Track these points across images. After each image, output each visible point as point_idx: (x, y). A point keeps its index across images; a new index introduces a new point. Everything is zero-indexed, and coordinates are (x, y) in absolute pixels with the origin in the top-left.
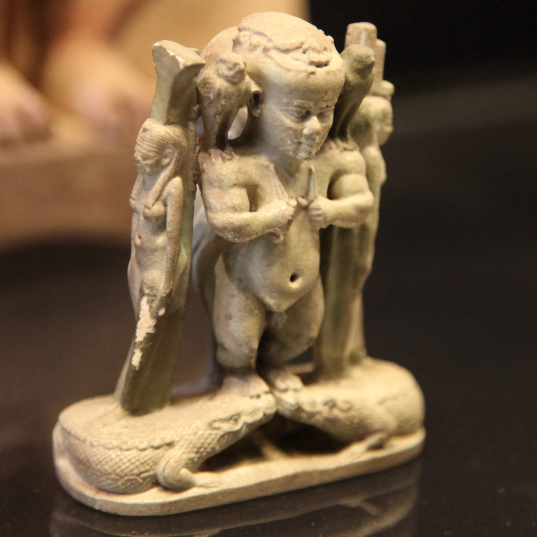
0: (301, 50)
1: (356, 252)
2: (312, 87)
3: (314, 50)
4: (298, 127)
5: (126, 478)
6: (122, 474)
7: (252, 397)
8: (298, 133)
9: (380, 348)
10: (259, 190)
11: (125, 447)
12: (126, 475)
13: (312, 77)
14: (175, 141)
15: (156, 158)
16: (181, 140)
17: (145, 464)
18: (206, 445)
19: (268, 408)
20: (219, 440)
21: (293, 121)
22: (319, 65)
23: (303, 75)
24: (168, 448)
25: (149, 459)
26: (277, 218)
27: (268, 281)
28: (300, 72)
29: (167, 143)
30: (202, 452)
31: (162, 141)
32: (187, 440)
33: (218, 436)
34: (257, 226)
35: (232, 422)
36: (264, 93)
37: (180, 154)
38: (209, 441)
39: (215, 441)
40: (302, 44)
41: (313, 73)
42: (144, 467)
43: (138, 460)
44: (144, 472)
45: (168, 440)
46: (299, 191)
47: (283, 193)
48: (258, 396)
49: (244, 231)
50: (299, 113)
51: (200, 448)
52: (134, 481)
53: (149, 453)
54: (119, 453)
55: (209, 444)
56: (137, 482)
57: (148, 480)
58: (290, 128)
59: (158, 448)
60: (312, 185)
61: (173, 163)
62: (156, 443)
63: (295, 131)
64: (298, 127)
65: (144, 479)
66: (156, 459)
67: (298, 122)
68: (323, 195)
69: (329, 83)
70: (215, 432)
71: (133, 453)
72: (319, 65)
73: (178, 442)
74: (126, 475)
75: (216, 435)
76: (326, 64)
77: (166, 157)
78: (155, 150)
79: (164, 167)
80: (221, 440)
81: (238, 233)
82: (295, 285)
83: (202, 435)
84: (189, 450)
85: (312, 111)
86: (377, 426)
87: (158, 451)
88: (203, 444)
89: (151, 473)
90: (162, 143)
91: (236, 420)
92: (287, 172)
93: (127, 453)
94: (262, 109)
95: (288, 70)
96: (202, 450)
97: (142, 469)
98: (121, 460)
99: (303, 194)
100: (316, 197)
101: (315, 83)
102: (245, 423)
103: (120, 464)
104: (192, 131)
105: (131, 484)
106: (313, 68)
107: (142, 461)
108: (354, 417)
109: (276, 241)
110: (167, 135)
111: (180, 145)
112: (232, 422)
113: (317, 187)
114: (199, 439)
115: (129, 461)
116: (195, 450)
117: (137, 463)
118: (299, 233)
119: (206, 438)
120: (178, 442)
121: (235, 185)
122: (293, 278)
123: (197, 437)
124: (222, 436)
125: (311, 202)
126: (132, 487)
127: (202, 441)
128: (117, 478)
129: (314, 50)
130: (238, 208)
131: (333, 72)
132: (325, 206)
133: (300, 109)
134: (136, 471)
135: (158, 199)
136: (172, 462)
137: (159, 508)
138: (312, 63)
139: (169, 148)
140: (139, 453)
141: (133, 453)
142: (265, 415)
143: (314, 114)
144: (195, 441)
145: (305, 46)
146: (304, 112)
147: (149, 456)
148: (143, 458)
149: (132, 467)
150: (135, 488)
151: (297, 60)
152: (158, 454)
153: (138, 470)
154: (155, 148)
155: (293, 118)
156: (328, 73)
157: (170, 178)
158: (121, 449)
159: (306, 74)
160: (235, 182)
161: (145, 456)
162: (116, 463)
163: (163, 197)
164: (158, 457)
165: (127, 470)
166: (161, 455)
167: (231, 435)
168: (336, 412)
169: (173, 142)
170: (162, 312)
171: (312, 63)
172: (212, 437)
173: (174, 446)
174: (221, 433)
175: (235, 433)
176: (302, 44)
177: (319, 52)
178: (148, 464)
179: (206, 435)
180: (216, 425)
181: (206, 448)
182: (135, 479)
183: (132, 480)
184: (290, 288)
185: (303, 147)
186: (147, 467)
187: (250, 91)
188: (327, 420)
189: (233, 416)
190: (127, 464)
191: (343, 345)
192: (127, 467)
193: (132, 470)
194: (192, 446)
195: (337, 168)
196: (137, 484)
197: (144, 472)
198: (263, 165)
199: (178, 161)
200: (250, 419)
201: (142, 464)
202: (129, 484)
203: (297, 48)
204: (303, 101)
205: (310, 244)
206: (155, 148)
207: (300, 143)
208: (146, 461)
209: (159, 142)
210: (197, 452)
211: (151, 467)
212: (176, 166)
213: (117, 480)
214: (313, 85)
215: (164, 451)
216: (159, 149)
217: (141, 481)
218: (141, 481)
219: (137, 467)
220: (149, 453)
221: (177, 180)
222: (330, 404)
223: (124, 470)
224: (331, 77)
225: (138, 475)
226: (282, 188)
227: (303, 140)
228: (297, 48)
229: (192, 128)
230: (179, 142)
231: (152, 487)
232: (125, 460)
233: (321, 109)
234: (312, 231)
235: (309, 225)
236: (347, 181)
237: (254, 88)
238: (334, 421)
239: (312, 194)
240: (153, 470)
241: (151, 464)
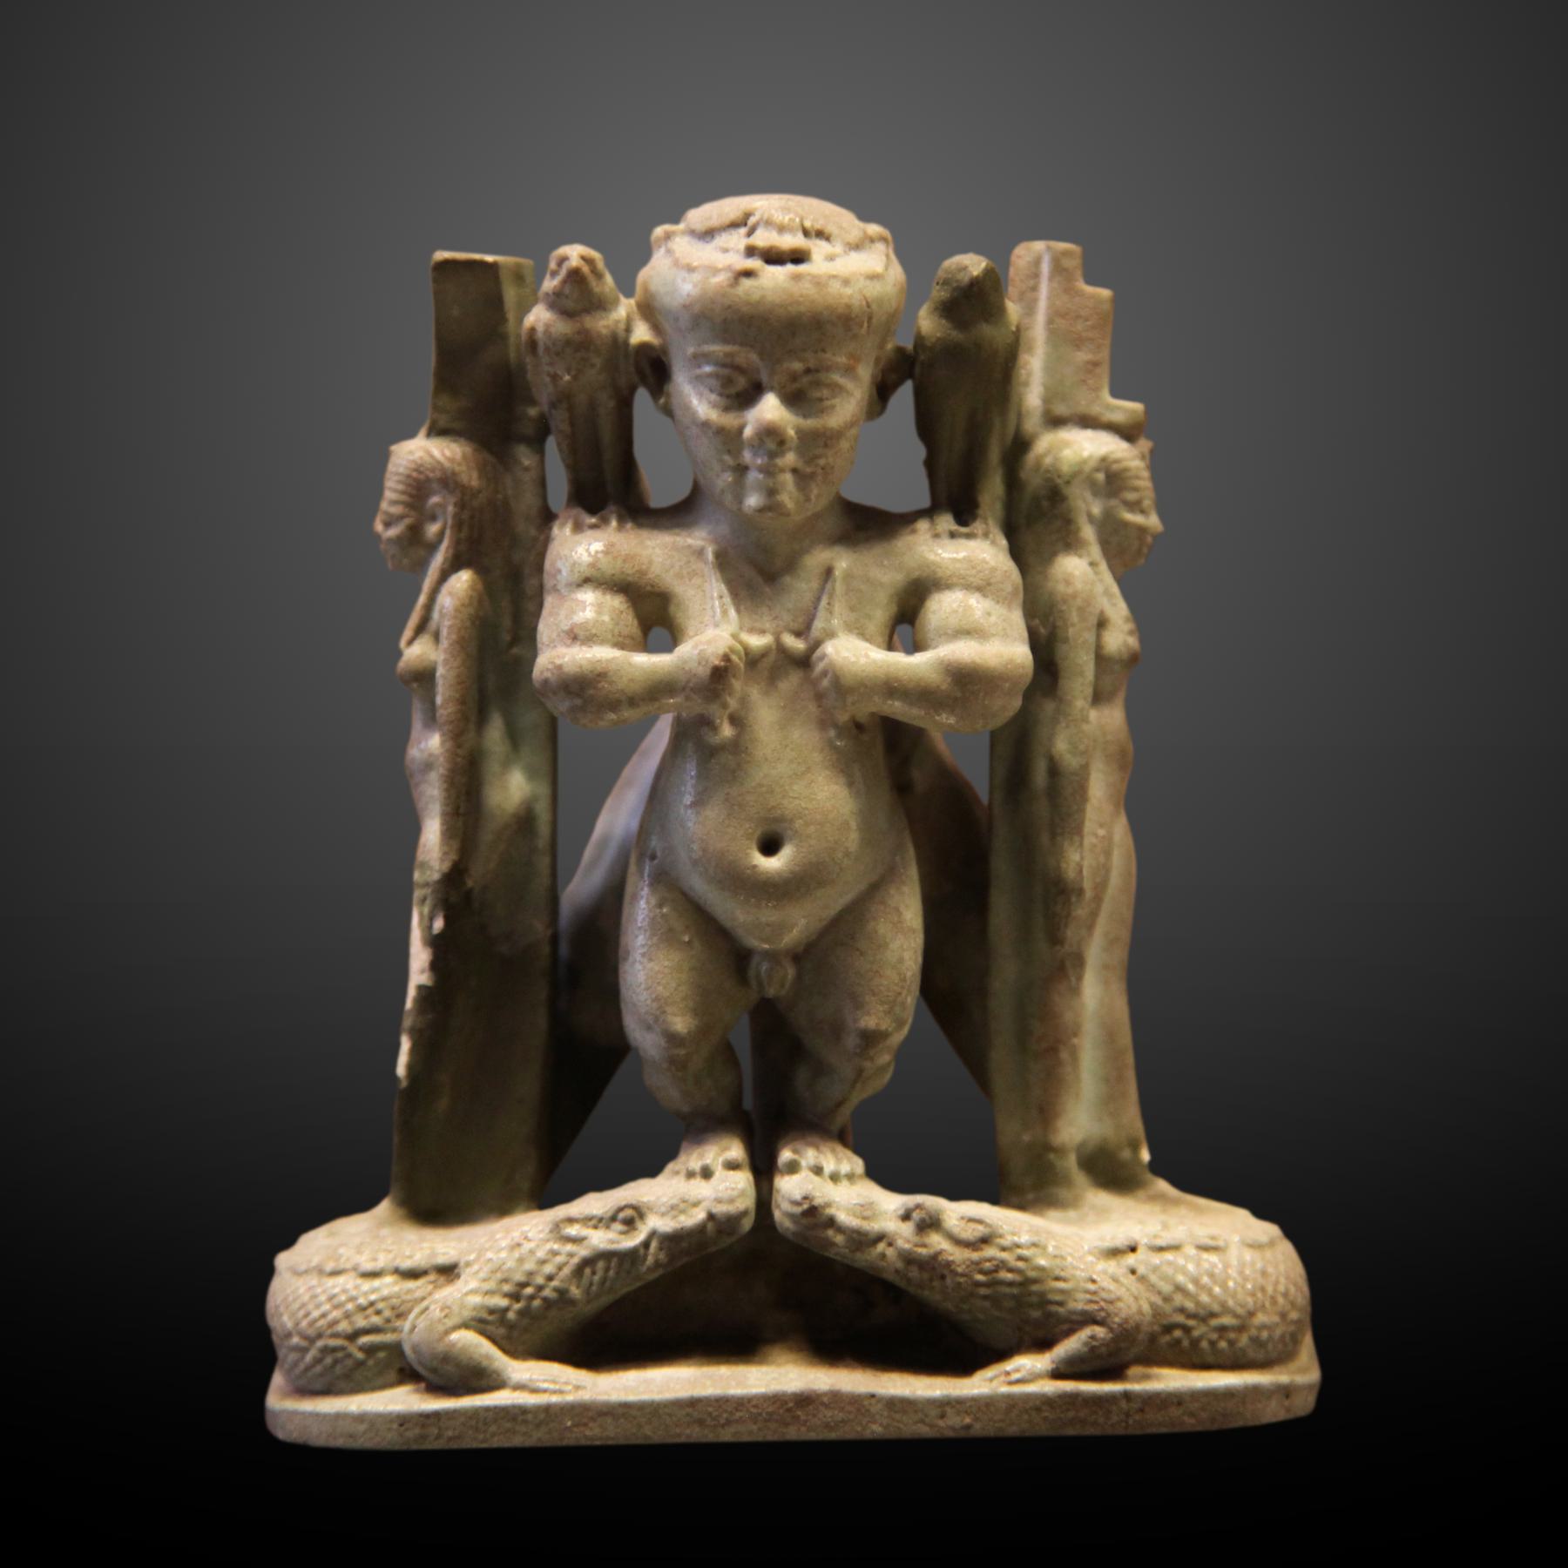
0: (743, 231)
1: (1045, 839)
2: (744, 309)
3: (769, 223)
4: (729, 420)
5: (320, 1343)
6: (311, 1332)
7: (690, 1175)
8: (730, 439)
9: (1195, 1155)
10: (672, 609)
11: (329, 1267)
12: (320, 1336)
13: (747, 283)
14: (443, 469)
15: (407, 521)
16: (457, 469)
17: (370, 1311)
18: (540, 1280)
19: (719, 1201)
20: (579, 1271)
21: (714, 406)
22: (774, 257)
23: (721, 279)
24: (442, 1279)
25: (384, 1299)
26: (685, 662)
27: (695, 847)
28: (715, 271)
29: (428, 480)
30: (532, 1298)
31: (415, 474)
32: (490, 1260)
33: (576, 1260)
34: (632, 680)
35: (618, 1226)
36: (664, 350)
37: (461, 505)
38: (548, 1269)
39: (567, 1271)
40: (748, 215)
41: (748, 274)
42: (366, 1317)
43: (352, 1299)
44: (367, 1331)
45: (441, 1260)
46: (787, 617)
47: (725, 612)
48: (707, 1173)
49: (592, 692)
50: (727, 382)
51: (523, 1285)
52: (340, 1355)
53: (388, 1286)
54: (314, 1282)
55: (550, 1278)
56: (349, 1356)
57: (381, 1355)
58: (706, 425)
59: (413, 1274)
60: (824, 602)
61: (448, 532)
62: (406, 1264)
63: (721, 431)
64: (729, 420)
65: (370, 1350)
66: (403, 1302)
67: (726, 409)
68: (863, 635)
69: (799, 303)
70: (569, 1247)
71: (346, 1283)
72: (774, 257)
73: (468, 1264)
74: (320, 1336)
75: (571, 1255)
76: (798, 257)
77: (433, 518)
78: (404, 498)
79: (432, 547)
80: (588, 1271)
81: (578, 695)
82: (772, 864)
83: (532, 1252)
84: (491, 1285)
85: (764, 377)
86: (1079, 1304)
87: (411, 1284)
88: (531, 1274)
89: (388, 1338)
90: (415, 480)
91: (630, 1223)
92: (756, 570)
93: (330, 1282)
94: (668, 396)
95: (690, 269)
96: (529, 1291)
97: (361, 1322)
98: (314, 1297)
99: (796, 626)
100: (831, 635)
101: (756, 297)
102: (653, 1234)
103: (310, 1307)
104: (527, 469)
105: (336, 1362)
106: (755, 263)
107: (362, 1301)
108: (1002, 1265)
109: (715, 740)
110: (427, 459)
111: (456, 483)
112: (618, 1226)
113: (838, 607)
114: (521, 1260)
115: (331, 1298)
116: (507, 1288)
117: (350, 1306)
118: (784, 725)
119: (543, 1262)
120: (468, 1264)
121: (586, 581)
122: (770, 846)
123: (516, 1255)
124: (588, 1262)
125: (817, 644)
126: (338, 1369)
127: (530, 1266)
128: (304, 1343)
129: (769, 223)
130: (581, 634)
131: (814, 277)
132: (854, 652)
133: (726, 371)
134: (343, 1326)
135: (421, 629)
136: (445, 1316)
137: (395, 1426)
138: (751, 251)
139: (434, 493)
140: (359, 1281)
141: (346, 1283)
142: (711, 1217)
143: (772, 389)
144: (510, 1264)
145: (752, 220)
146: (741, 382)
147: (385, 1292)
148: (366, 1294)
149: (335, 1314)
150: (347, 1376)
151: (726, 251)
152: (409, 1291)
153: (351, 1323)
154: (403, 493)
155: (713, 397)
156: (797, 278)
157: (444, 576)
158: (320, 1271)
159: (729, 275)
160: (588, 573)
161: (374, 1291)
162: (303, 1305)
163: (433, 625)
164: (409, 1297)
165: (322, 1322)
166: (418, 1294)
167: (614, 1262)
168: (937, 1242)
169: (438, 474)
170: (439, 924)
171: (751, 251)
172: (559, 1259)
173: (458, 1276)
174: (583, 1252)
175: (630, 1258)
176: (748, 215)
177: (782, 229)
178: (378, 1313)
179: (541, 1254)
180: (573, 1230)
181: (540, 1288)
182: (343, 1348)
183: (334, 1350)
184: (755, 866)
185: (753, 476)
186: (376, 1320)
187: (626, 343)
188: (909, 1259)
189: (621, 1209)
190: (327, 1307)
191: (1046, 1112)
192: (324, 1315)
193: (335, 1322)
194: (499, 1276)
195: (916, 574)
196: (349, 1362)
197: (367, 1331)
198: (690, 546)
199: (458, 525)
200: (665, 1225)
201: (362, 1309)
202: (329, 1360)
203: (734, 225)
204: (728, 348)
205: (817, 757)
206: (403, 493)
207: (741, 470)
208: (372, 1304)
209: (409, 476)
210: (515, 1297)
211: (388, 1321)
212: (457, 543)
213: (303, 1351)
214: (748, 303)
215: (431, 1287)
216: (411, 496)
217: (360, 1356)
218: (360, 1356)
219: (347, 1316)
220: (388, 1286)
221: (463, 580)
222: (916, 1215)
223: (316, 1321)
224: (807, 288)
225: (353, 1336)
226: (727, 599)
227: (747, 456)
228: (734, 225)
229: (526, 463)
230: (454, 474)
231: (400, 1382)
232: (323, 1298)
233: (794, 377)
234: (824, 723)
235: (812, 708)
236: (943, 607)
237: (641, 334)
238: (934, 1266)
239: (818, 624)
240: (394, 1330)
241: (387, 1313)
